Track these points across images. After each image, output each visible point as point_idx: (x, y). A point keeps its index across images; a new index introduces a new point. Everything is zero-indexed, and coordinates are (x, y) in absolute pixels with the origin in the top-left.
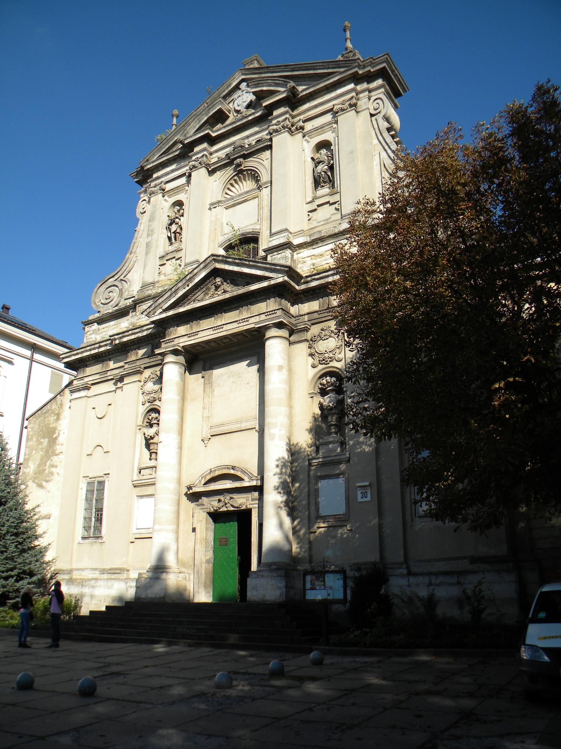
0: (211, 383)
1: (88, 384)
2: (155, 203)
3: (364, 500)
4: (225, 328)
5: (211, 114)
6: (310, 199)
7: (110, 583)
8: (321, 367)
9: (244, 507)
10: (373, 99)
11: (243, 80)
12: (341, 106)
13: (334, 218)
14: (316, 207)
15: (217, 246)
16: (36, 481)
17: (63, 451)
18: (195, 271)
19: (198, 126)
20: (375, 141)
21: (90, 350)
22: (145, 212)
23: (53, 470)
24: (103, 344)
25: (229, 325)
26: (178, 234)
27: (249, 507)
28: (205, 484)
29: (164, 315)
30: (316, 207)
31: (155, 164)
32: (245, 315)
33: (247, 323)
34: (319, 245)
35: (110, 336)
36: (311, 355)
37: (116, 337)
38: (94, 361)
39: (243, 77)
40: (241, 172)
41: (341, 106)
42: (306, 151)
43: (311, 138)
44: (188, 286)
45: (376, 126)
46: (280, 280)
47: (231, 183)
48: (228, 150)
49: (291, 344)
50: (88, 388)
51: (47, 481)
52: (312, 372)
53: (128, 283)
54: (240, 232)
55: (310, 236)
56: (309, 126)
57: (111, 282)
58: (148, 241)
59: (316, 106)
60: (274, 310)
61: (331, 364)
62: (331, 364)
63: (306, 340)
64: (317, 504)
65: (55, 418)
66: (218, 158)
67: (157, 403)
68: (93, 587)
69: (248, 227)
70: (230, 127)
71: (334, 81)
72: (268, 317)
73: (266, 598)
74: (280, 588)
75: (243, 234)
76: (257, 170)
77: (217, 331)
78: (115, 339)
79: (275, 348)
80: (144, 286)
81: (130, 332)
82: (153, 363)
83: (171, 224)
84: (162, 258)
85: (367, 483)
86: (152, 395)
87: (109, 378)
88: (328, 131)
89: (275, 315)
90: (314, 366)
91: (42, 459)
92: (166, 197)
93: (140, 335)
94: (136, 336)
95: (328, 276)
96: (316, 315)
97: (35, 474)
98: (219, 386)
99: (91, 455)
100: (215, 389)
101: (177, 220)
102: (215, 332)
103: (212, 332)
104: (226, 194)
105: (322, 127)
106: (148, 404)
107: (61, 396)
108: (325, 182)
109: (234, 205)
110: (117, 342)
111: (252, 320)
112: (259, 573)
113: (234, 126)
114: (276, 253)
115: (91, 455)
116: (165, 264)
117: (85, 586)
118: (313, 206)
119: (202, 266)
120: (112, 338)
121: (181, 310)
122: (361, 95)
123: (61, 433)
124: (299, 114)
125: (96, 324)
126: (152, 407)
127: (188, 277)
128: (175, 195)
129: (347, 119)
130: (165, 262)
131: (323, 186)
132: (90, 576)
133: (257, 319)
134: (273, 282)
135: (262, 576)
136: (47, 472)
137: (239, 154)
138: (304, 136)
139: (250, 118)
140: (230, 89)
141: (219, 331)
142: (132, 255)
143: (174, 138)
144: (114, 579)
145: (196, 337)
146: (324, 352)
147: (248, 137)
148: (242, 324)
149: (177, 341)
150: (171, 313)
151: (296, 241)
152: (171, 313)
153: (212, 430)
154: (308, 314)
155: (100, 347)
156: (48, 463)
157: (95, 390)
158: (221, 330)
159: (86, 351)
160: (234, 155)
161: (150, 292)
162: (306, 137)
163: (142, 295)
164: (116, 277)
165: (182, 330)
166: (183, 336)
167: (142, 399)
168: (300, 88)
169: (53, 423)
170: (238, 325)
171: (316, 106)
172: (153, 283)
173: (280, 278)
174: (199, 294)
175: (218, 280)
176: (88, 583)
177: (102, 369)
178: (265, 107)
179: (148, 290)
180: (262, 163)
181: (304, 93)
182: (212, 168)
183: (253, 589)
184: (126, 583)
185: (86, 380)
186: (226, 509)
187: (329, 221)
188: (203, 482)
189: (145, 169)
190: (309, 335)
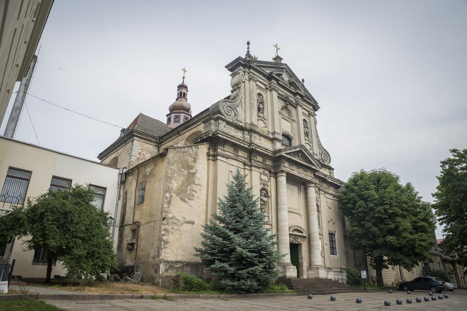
4: (302, 174)
11: (285, 68)
16: (180, 196)
21: (236, 141)
23: (194, 193)
29: (286, 156)
40: (286, 107)
47: (282, 109)
48: (282, 93)
50: (227, 158)
51: (190, 199)
59: (306, 106)
65: (193, 160)
78: (253, 146)
91: (183, 182)
93: (264, 152)
94: (263, 151)
97: (178, 190)
109: (284, 119)
110: (254, 148)
111: (308, 177)
123: (198, 172)
136: (188, 192)
152: (289, 157)
155: (242, 143)
156: (189, 187)
159: (234, 139)
165: (287, 164)
166: (286, 167)
171: (306, 106)
180: (293, 111)
185: (226, 153)
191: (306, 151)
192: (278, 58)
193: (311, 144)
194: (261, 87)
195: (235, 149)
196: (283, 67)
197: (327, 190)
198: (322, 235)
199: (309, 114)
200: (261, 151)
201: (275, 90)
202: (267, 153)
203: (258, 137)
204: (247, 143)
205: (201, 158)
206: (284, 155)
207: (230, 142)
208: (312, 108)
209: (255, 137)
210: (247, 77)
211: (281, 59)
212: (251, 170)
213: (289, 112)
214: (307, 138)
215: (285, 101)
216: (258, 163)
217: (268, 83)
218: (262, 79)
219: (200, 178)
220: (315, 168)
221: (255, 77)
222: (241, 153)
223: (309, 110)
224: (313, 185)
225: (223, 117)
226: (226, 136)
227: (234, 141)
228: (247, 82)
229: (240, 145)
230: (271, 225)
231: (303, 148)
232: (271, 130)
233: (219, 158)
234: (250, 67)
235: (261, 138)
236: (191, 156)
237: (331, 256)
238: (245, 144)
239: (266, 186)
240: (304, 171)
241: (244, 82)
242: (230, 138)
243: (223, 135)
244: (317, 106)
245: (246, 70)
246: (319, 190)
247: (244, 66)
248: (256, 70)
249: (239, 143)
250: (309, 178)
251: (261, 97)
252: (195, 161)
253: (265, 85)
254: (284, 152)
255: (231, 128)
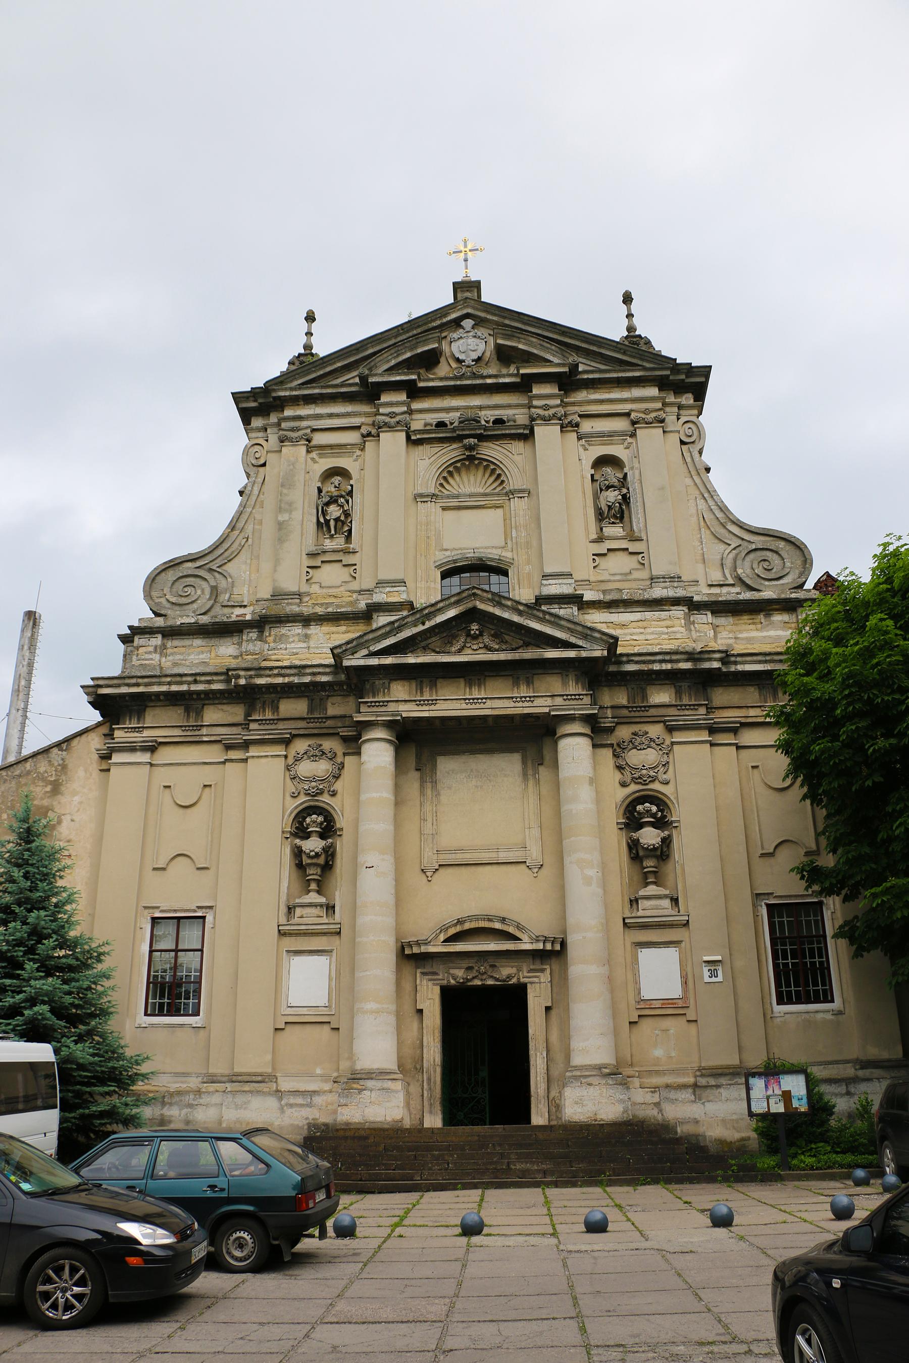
0: (434, 783)
1: (156, 741)
2: (292, 459)
3: (714, 979)
4: (489, 703)
5: (419, 351)
6: (594, 536)
7: (240, 1099)
8: (633, 787)
9: (514, 981)
10: (683, 419)
11: (467, 316)
12: (643, 416)
13: (636, 575)
14: (606, 552)
15: (432, 566)
17: (73, 854)
18: (441, 605)
19: (393, 362)
20: (688, 481)
21: (169, 684)
22: (264, 465)
24: (203, 678)
25: (496, 701)
26: (340, 524)
27: (522, 980)
28: (446, 941)
29: (374, 661)
30: (606, 552)
31: (294, 393)
32: (524, 691)
33: (530, 704)
34: (619, 610)
35: (228, 670)
36: (620, 768)
37: (242, 673)
38: (168, 703)
39: (470, 311)
40: (471, 458)
41: (643, 416)
42: (584, 462)
43: (589, 445)
44: (423, 624)
45: (688, 460)
46: (598, 654)
47: (451, 471)
48: (445, 417)
49: (594, 746)
52: (623, 792)
53: (229, 580)
54: (476, 555)
55: (604, 592)
56: (587, 426)
57: (189, 568)
58: (280, 518)
59: (602, 402)
60: (579, 695)
61: (651, 786)
62: (651, 786)
63: (612, 745)
64: (637, 982)
65: (49, 788)
66: (426, 425)
67: (326, 798)
68: (190, 1106)
69: (489, 551)
70: (452, 383)
71: (634, 377)
72: (567, 702)
73: (599, 1117)
74: (621, 1101)
75: (480, 559)
76: (501, 465)
77: (473, 706)
78: (238, 677)
79: (575, 751)
80: (278, 596)
81: (276, 671)
82: (316, 731)
83: (328, 504)
84: (311, 555)
85: (719, 958)
86: (314, 784)
87: (205, 739)
88: (617, 444)
89: (580, 702)
90: (623, 785)
92: (314, 455)
93: (296, 680)
94: (287, 680)
95: (654, 662)
96: (625, 712)
98: (450, 788)
99: (164, 869)
100: (442, 792)
101: (342, 500)
102: (469, 706)
103: (464, 706)
104: (441, 485)
105: (611, 434)
106: (303, 798)
107: (62, 750)
108: (616, 518)
109: (459, 508)
110: (242, 682)
111: (538, 702)
112: (584, 1081)
113: (458, 383)
114: (556, 606)
115: (164, 869)
116: (319, 567)
117: (171, 1104)
118: (602, 548)
119: (453, 600)
120: (227, 674)
121: (411, 659)
122: (668, 409)
123: (66, 820)
124: (573, 404)
125: (160, 636)
126: (312, 803)
127: (426, 611)
128: (333, 457)
129: (649, 437)
130: (319, 564)
131: (613, 523)
132: (174, 1087)
133: (549, 702)
134: (584, 654)
135: (590, 1085)
137: (473, 432)
138: (579, 439)
139: (489, 381)
140: (445, 320)
141: (478, 706)
142: (236, 532)
143: (334, 363)
144: (251, 1092)
145: (432, 707)
146: (640, 767)
147: (481, 408)
148: (521, 704)
149: (392, 707)
150: (389, 660)
151: (588, 596)
152: (389, 660)
153: (441, 857)
154: (612, 707)
155: (196, 682)
157: (166, 755)
158: (482, 706)
159: (160, 684)
160: (463, 430)
161: (293, 608)
162: (583, 442)
163: (275, 610)
164: (198, 564)
165: (399, 690)
167: (290, 787)
168: (581, 368)
169: (42, 799)
170: (513, 704)
171: (602, 402)
172: (300, 595)
173: (599, 652)
174: (435, 641)
175: (475, 627)
176: (176, 1099)
177: (188, 721)
178: (522, 374)
179: (291, 604)
181: (585, 376)
182: (418, 436)
183: (576, 1103)
184: (280, 1099)
185: (146, 733)
186: (479, 983)
187: (629, 577)
188: (442, 937)
189: (274, 394)
190: (612, 740)
191: (499, 604)
192: (466, 289)
193: (633, 547)
194: (331, 447)
195: (187, 710)
196: (454, 316)
197: (752, 712)
198: (687, 924)
199: (634, 423)
200: (280, 680)
201: (390, 427)
202: (307, 679)
203: (298, 629)
204: (216, 674)
205: (81, 773)
206: (362, 662)
207: (158, 695)
208: (653, 391)
209: (280, 639)
210: (273, 438)
211: (477, 285)
212: (245, 760)
213: (494, 471)
214: (615, 530)
215: (460, 438)
216: (281, 725)
217: (367, 415)
218: (338, 416)
219: (72, 837)
220: (571, 654)
221: (304, 424)
222: (211, 715)
223: (626, 407)
224: (577, 727)
225: (160, 622)
226: (128, 685)
227: (164, 688)
228: (272, 459)
229: (190, 693)
230: (339, 933)
231: (482, 600)
232: (368, 584)
233: (117, 758)
234: (280, 404)
235: (314, 630)
236: (44, 779)
237: (780, 1009)
238: (209, 682)
239: (326, 798)
240: (516, 684)
241: (264, 465)
242: (146, 685)
243: (119, 686)
244: (689, 369)
245: (273, 418)
246: (670, 730)
247: (264, 410)
248: (310, 400)
249: (184, 688)
250: (541, 706)
251: (337, 480)
252: (56, 788)
253: (359, 428)
254: (365, 652)
255: (187, 642)
